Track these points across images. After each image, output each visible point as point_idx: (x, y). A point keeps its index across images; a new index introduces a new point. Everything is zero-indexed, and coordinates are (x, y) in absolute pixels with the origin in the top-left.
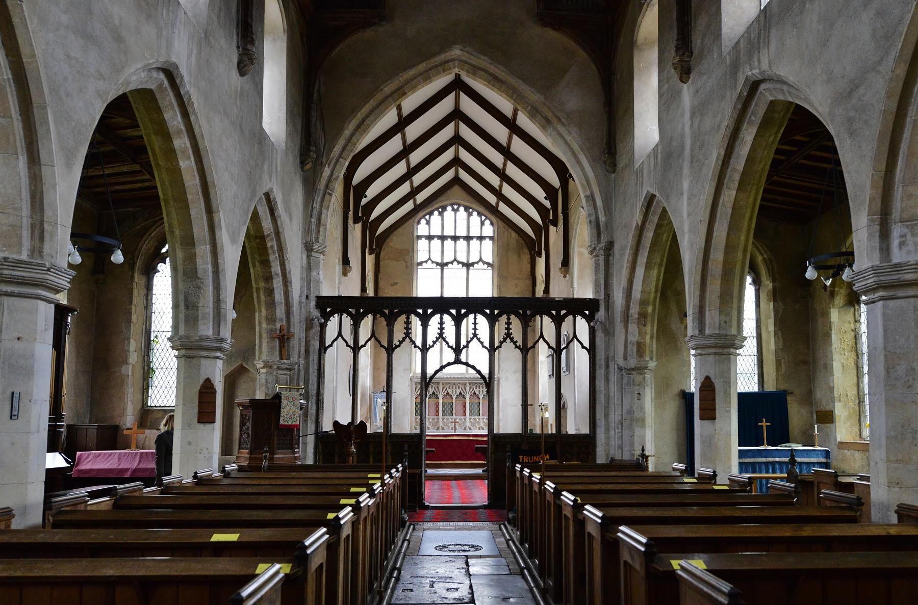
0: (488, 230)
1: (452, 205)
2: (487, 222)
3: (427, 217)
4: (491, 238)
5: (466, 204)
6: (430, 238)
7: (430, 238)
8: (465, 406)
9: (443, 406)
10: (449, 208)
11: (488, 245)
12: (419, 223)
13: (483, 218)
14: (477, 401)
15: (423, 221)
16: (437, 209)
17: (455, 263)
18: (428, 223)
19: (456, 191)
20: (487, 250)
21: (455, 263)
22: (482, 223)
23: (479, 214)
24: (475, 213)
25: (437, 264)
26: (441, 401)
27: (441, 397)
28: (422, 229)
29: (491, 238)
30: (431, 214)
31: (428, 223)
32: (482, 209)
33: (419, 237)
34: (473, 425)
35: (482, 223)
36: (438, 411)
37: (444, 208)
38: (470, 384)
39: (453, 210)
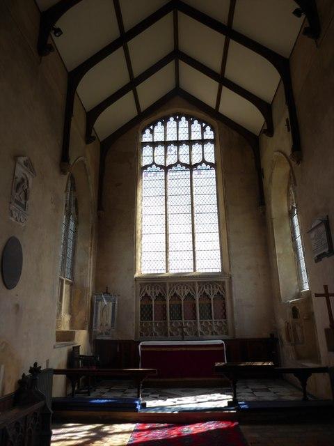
0: (209, 134)
1: (174, 116)
2: (208, 128)
3: (151, 127)
4: (212, 141)
5: (187, 111)
6: (154, 144)
7: (154, 144)
8: (194, 309)
9: (171, 309)
10: (172, 119)
11: (210, 148)
12: (143, 132)
13: (204, 125)
14: (207, 302)
15: (148, 131)
16: (160, 120)
17: (179, 166)
18: (152, 132)
19: (178, 103)
20: (210, 152)
21: (179, 166)
22: (203, 130)
23: (200, 122)
24: (196, 122)
25: (161, 167)
26: (168, 303)
27: (168, 298)
28: (147, 137)
29: (212, 141)
30: (155, 124)
31: (152, 132)
32: (202, 115)
33: (145, 144)
34: (205, 329)
35: (203, 130)
36: (165, 315)
37: (167, 119)
38: (199, 283)
39: (175, 119)
